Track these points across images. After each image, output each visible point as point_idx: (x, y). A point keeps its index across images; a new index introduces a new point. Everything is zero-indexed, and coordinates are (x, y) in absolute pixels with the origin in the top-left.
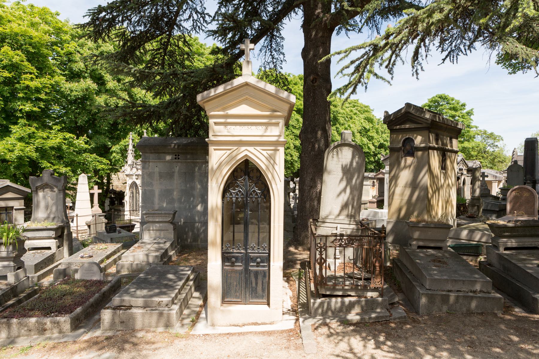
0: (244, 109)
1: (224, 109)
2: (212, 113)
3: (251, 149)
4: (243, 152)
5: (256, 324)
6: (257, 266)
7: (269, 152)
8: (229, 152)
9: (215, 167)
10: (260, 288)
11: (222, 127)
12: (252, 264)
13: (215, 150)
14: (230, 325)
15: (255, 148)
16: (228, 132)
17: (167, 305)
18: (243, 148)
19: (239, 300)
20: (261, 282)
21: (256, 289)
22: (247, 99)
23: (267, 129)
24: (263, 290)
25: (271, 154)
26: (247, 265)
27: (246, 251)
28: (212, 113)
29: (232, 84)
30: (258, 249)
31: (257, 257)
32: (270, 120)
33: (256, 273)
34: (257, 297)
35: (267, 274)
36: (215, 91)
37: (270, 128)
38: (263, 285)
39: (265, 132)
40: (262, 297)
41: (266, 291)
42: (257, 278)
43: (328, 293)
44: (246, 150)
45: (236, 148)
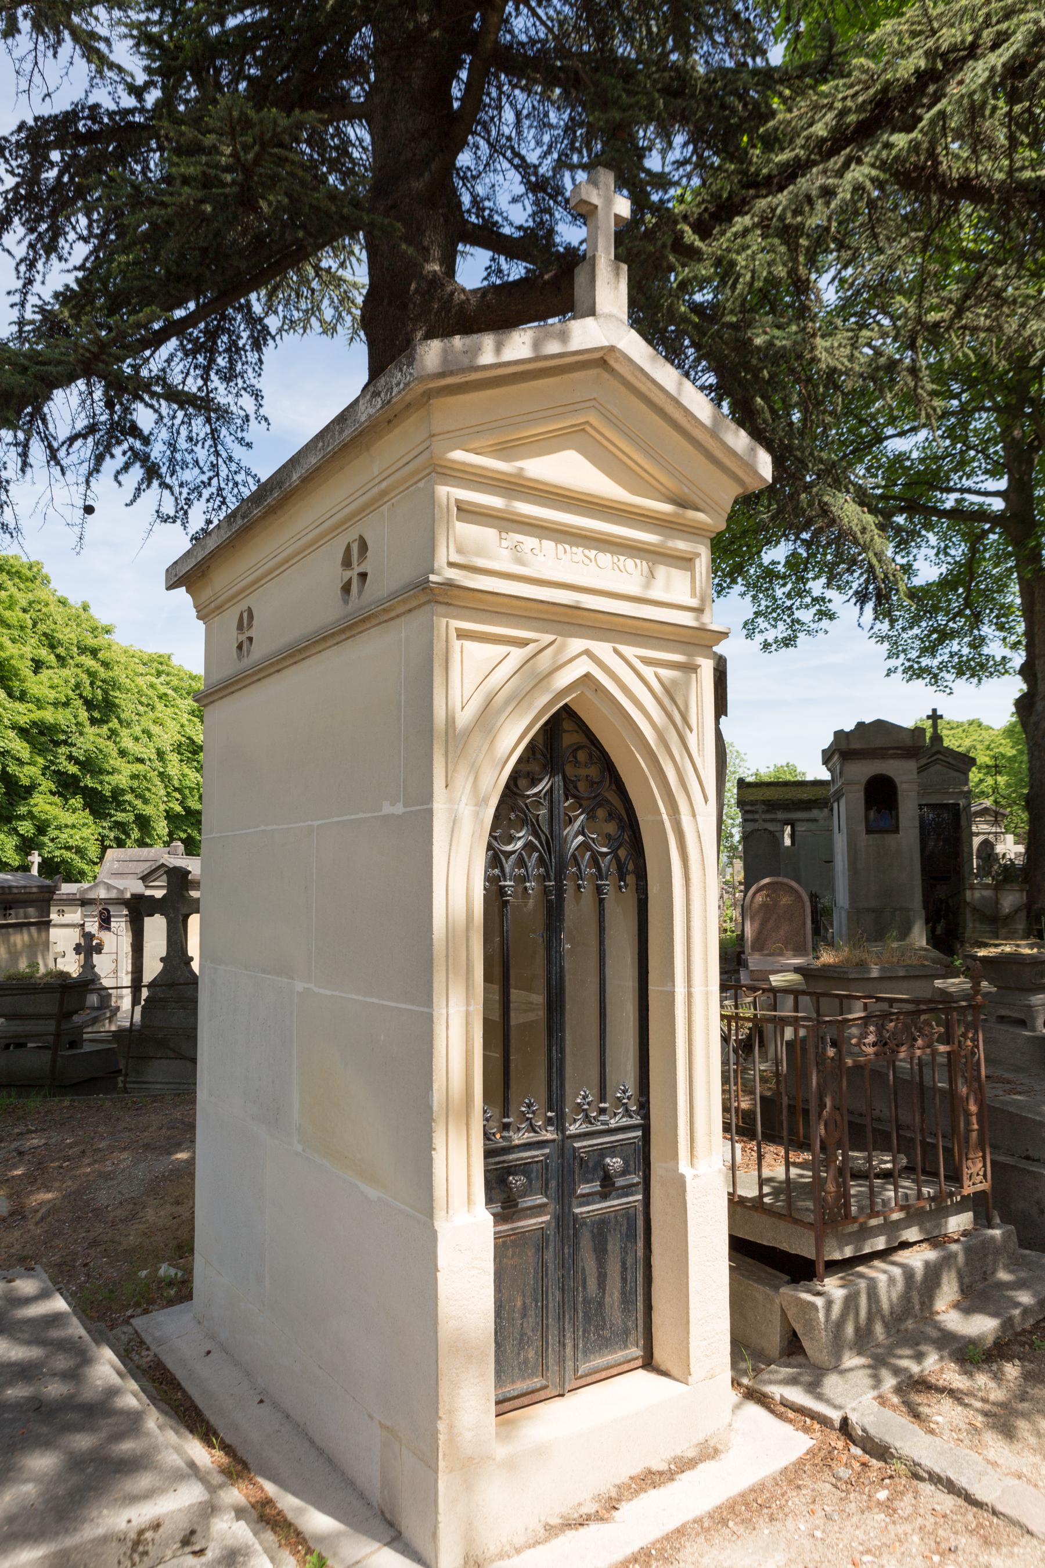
0: (567, 468)
1: (503, 450)
2: (458, 455)
3: (603, 649)
4: (577, 660)
5: (650, 1479)
6: (604, 1196)
7: (666, 673)
8: (518, 655)
9: (464, 718)
10: (613, 1296)
11: (487, 534)
12: (583, 1189)
13: (462, 635)
14: (552, 1531)
15: (621, 648)
16: (520, 562)
17: (186, 1542)
18: (577, 644)
19: (537, 1382)
20: (618, 1266)
21: (601, 1304)
22: (580, 430)
23: (652, 575)
24: (627, 1300)
25: (674, 682)
26: (565, 1196)
27: (561, 1128)
28: (458, 455)
29: (564, 336)
30: (602, 1111)
31: (603, 1152)
32: (668, 537)
33: (601, 1227)
34: (606, 1344)
35: (640, 1223)
36: (498, 349)
37: (662, 571)
38: (624, 1280)
39: (647, 586)
40: (623, 1338)
41: (640, 1305)
42: (605, 1251)
43: (848, 1252)
44: (587, 652)
45: (552, 637)
